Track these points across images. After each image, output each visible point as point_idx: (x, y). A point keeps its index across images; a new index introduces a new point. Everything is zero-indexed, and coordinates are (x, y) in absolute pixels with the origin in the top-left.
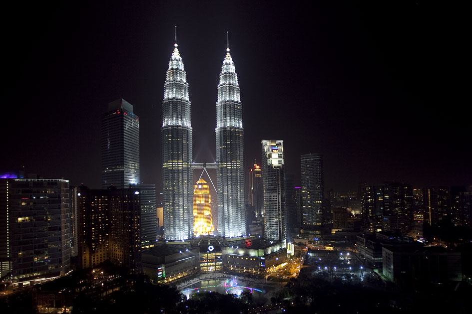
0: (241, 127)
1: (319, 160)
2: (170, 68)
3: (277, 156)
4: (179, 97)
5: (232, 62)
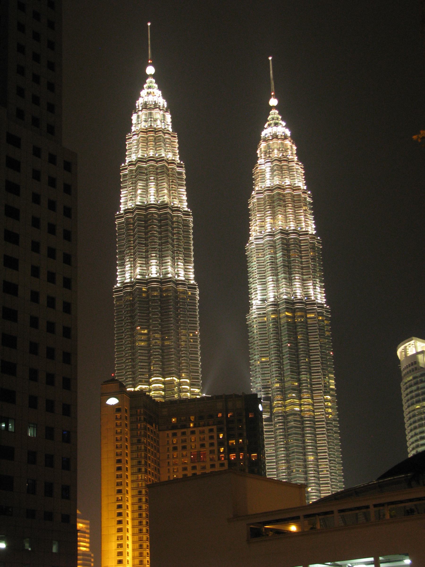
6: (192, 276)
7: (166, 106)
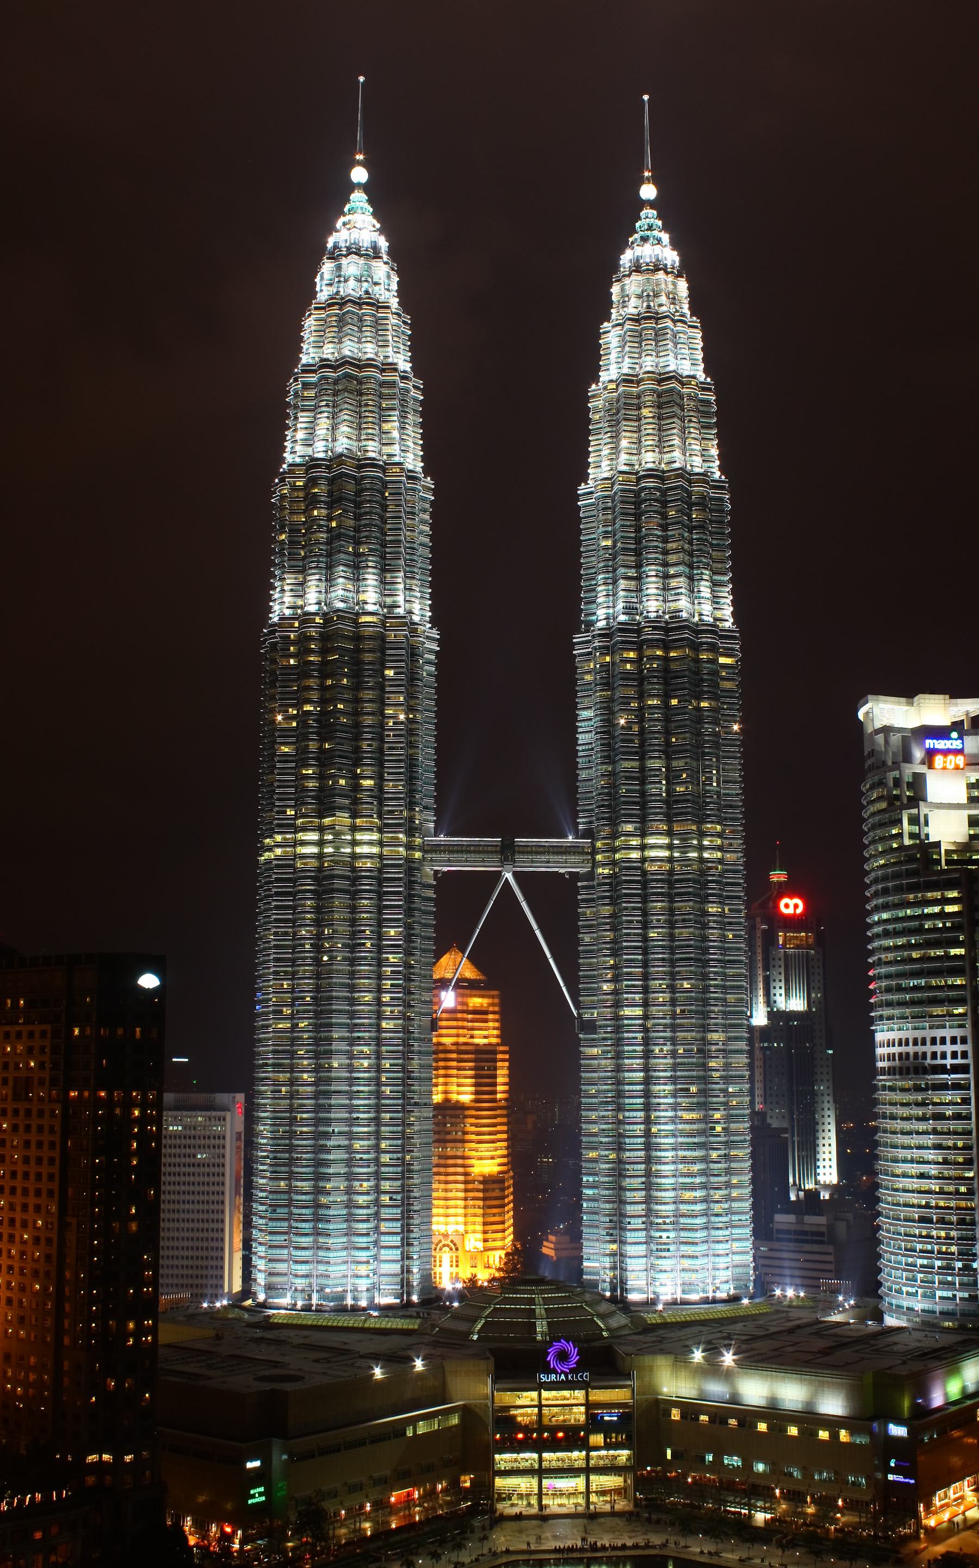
0: (728, 625)
4: (372, 449)
5: (671, 257)
6: (727, 611)
7: (677, 264)
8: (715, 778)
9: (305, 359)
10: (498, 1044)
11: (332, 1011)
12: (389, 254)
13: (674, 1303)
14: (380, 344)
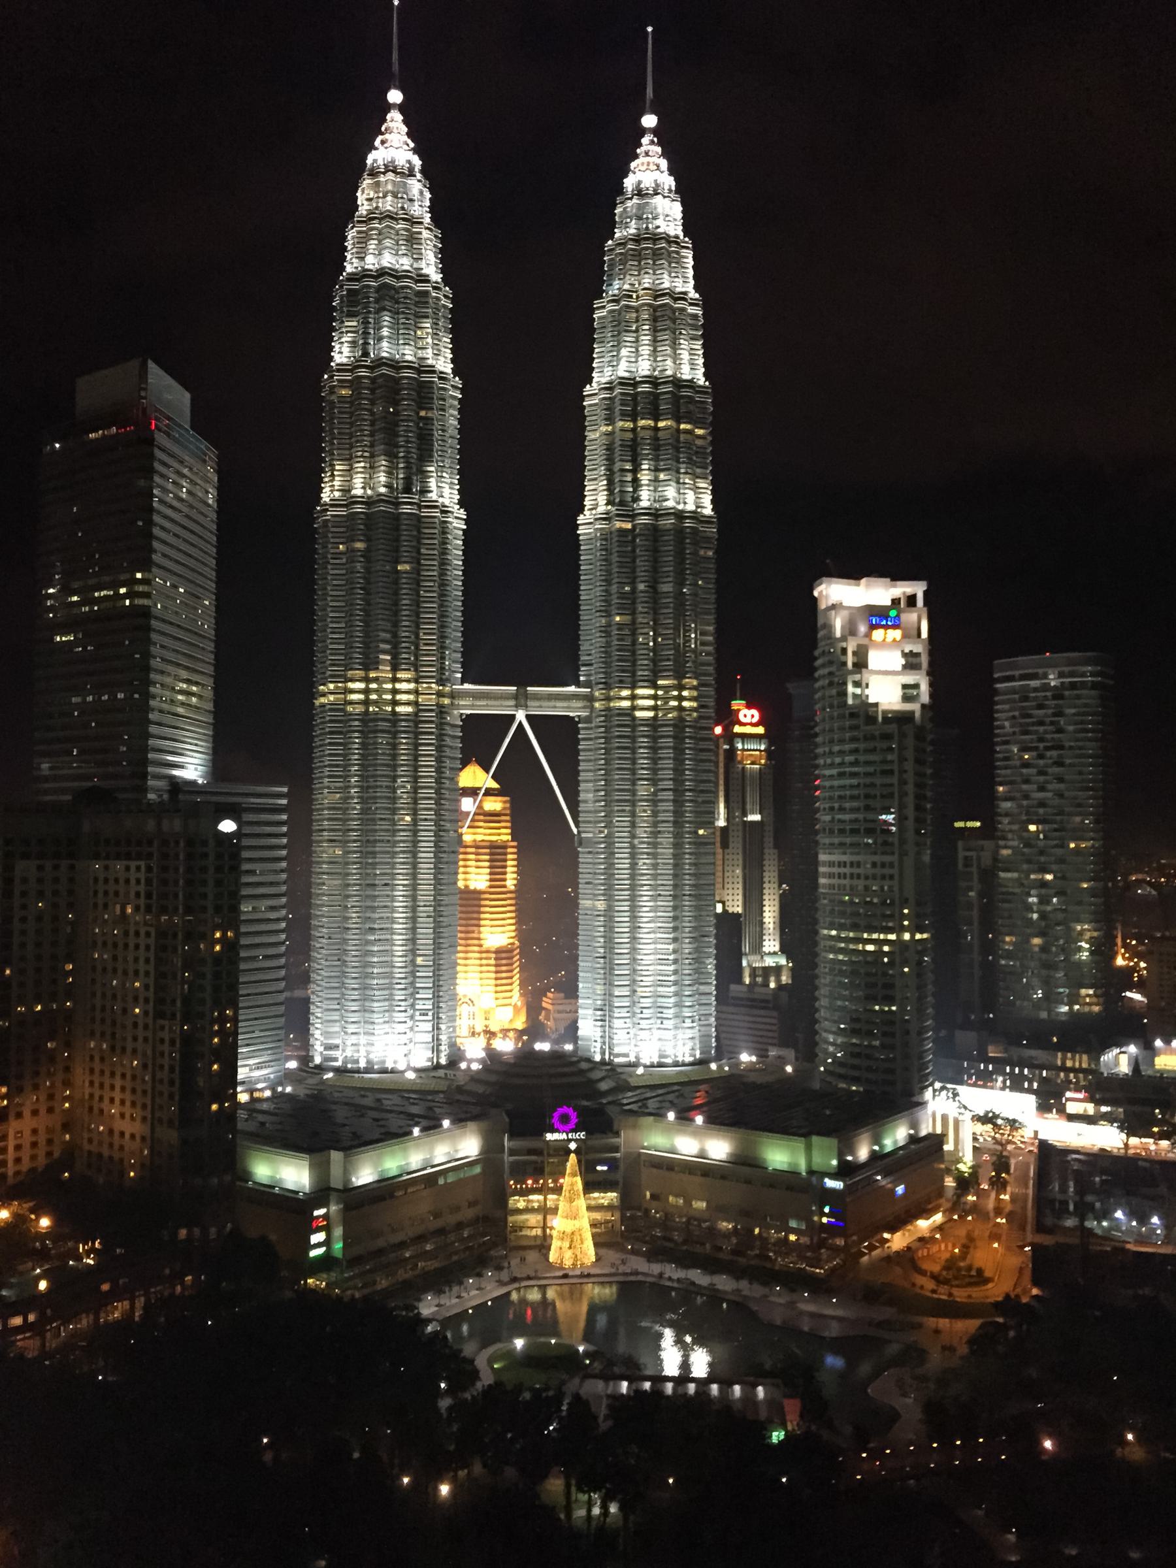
0: (708, 511)
1: (1094, 686)
2: (363, 208)
3: (897, 661)
4: (409, 354)
5: (669, 182)
6: (707, 499)
8: (693, 641)
9: (349, 269)
10: (508, 841)
11: (376, 831)
12: (422, 172)
13: (652, 1066)
14: (415, 256)
